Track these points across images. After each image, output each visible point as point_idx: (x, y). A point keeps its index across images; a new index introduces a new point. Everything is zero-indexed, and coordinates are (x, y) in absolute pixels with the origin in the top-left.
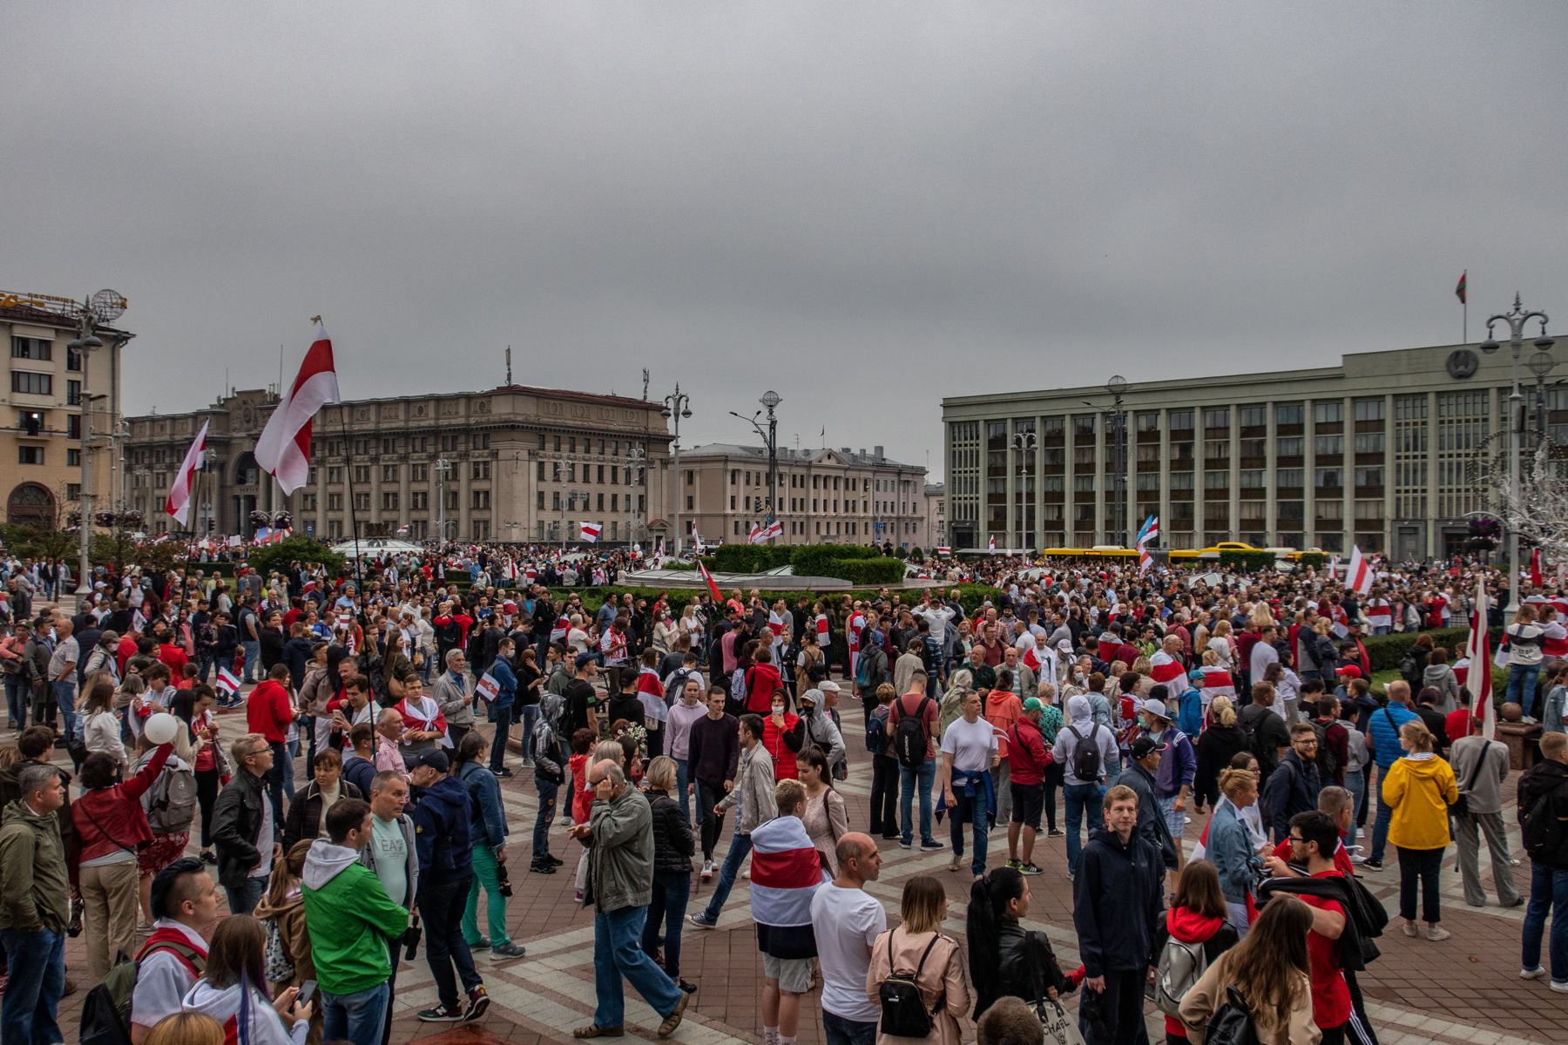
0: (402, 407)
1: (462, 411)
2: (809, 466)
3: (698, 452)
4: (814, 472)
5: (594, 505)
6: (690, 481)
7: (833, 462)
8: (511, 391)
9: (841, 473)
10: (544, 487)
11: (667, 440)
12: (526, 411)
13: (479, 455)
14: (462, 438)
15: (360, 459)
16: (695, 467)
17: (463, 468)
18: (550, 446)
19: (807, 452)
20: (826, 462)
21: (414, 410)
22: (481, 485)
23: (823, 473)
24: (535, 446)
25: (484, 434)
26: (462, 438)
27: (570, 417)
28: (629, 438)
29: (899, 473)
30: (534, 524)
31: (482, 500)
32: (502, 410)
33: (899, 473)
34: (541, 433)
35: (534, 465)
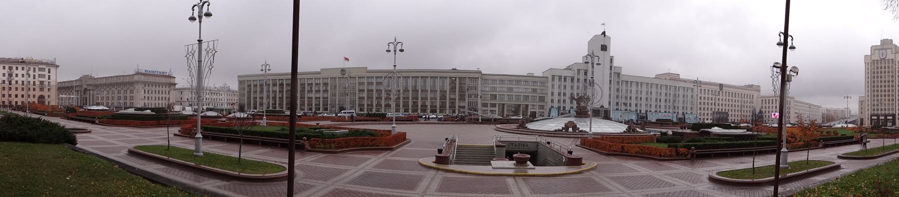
0: (116, 78)
1: (128, 79)
2: (210, 90)
3: (184, 87)
4: (211, 92)
5: (157, 99)
6: (182, 94)
7: (216, 89)
8: (138, 74)
9: (218, 92)
10: (145, 95)
11: (175, 84)
12: (143, 78)
13: (131, 88)
14: (128, 85)
15: (108, 89)
16: (181, 91)
17: (128, 91)
18: (147, 86)
19: (210, 87)
20: (214, 89)
21: (118, 78)
22: (132, 95)
23: (214, 92)
24: (144, 86)
25: (132, 84)
26: (128, 85)
27: (152, 79)
28: (163, 84)
29: (233, 92)
30: (143, 103)
31: (132, 98)
32: (136, 78)
33: (233, 92)
34: (145, 83)
35: (143, 91)
